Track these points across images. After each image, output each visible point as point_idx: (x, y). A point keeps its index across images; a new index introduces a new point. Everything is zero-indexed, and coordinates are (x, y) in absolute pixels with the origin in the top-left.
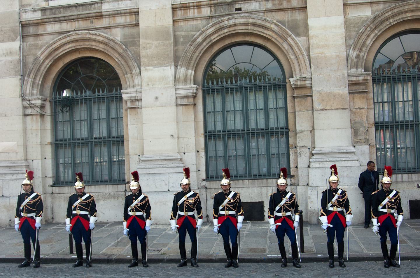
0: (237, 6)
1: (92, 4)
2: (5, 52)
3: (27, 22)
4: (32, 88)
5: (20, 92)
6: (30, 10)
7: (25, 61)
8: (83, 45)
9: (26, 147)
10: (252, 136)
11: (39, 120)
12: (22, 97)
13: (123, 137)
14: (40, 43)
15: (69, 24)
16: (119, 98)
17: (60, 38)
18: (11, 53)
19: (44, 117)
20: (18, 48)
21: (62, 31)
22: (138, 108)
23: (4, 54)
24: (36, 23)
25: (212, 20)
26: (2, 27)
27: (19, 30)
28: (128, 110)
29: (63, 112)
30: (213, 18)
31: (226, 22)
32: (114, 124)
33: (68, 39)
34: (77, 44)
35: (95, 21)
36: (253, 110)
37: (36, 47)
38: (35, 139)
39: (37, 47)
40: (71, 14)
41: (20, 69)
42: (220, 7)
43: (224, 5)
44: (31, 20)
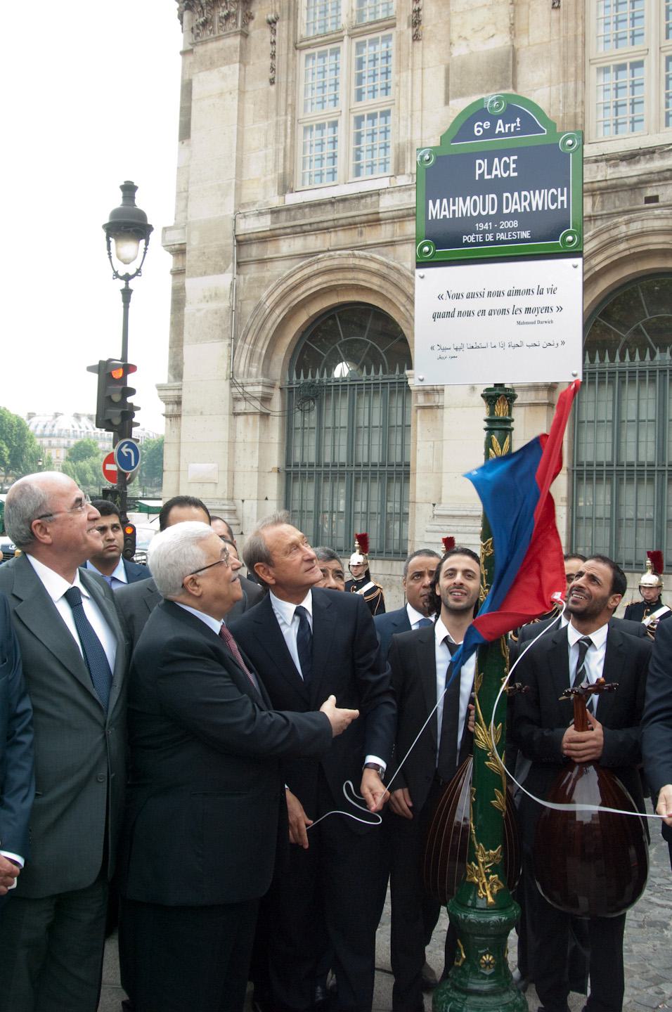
0: (650, 192)
1: (362, 197)
2: (207, 294)
3: (247, 236)
4: (249, 362)
5: (227, 369)
6: (252, 213)
7: (241, 310)
8: (343, 279)
9: (232, 474)
10: (596, 478)
11: (258, 423)
12: (231, 379)
13: (408, 465)
14: (267, 275)
15: (319, 239)
16: (403, 389)
17: (302, 266)
18: (216, 296)
19: (268, 419)
20: (229, 286)
21: (307, 251)
22: (438, 407)
23: (205, 297)
24: (262, 238)
25: (594, 224)
26: (204, 247)
27: (232, 251)
28: (419, 411)
30: (596, 219)
31: (623, 228)
32: (396, 439)
33: (315, 267)
34: (332, 277)
35: (366, 231)
37: (261, 283)
38: (248, 460)
39: (263, 284)
40: (322, 218)
41: (230, 326)
42: (613, 196)
43: (621, 191)
44: (253, 233)
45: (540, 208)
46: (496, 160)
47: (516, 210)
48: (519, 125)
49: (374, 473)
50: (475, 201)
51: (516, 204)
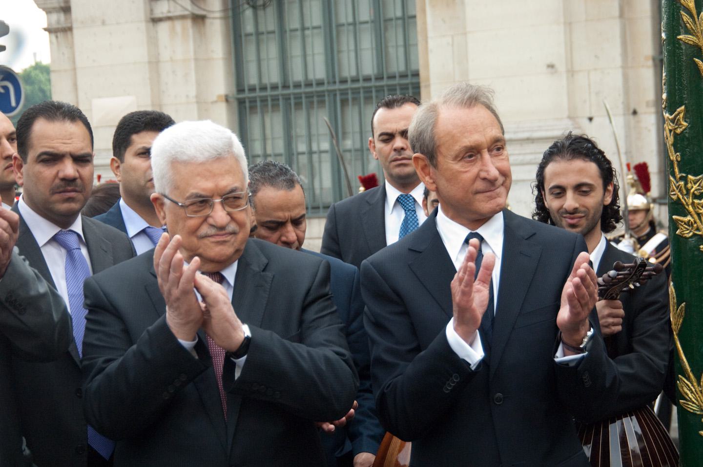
13: (416, 74)
29: (255, 8)
32: (394, 37)
36: (366, 22)
49: (368, 90)
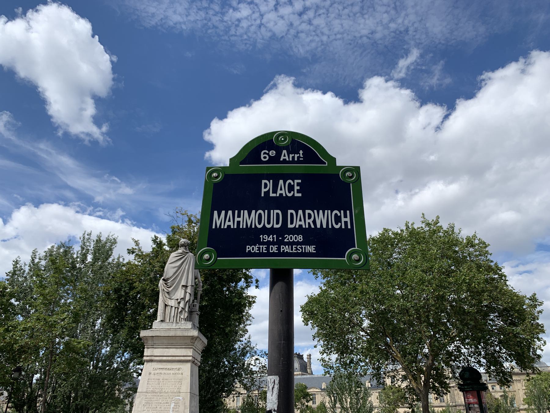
45: (325, 226)
46: (281, 182)
47: (300, 226)
48: (301, 156)
50: (260, 215)
51: (300, 220)
